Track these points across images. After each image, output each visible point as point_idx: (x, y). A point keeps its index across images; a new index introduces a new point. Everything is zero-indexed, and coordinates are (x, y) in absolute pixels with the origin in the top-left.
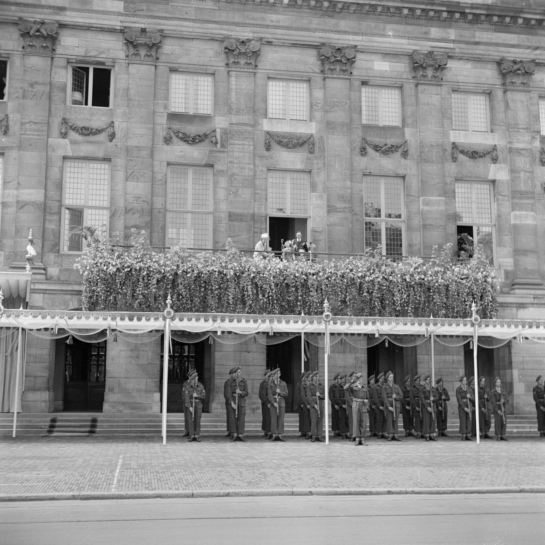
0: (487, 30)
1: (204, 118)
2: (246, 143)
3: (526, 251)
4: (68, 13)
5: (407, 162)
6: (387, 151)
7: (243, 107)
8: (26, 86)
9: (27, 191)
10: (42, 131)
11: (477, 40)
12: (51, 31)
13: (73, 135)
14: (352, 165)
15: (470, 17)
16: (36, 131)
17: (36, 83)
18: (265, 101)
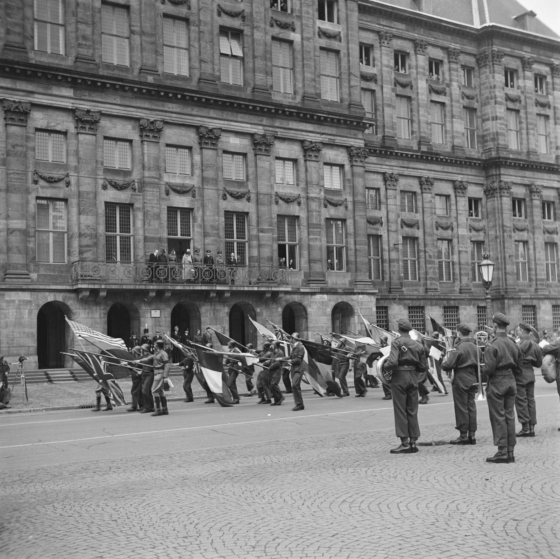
0: (296, 121)
1: (127, 173)
2: (155, 190)
3: (316, 260)
4: (36, 96)
5: (250, 204)
6: (238, 197)
7: (152, 166)
8: (10, 147)
9: (15, 221)
10: (23, 179)
11: (290, 127)
12: (26, 109)
13: (42, 183)
14: (218, 206)
15: (287, 113)
16: (18, 179)
17: (17, 145)
18: (165, 161)
